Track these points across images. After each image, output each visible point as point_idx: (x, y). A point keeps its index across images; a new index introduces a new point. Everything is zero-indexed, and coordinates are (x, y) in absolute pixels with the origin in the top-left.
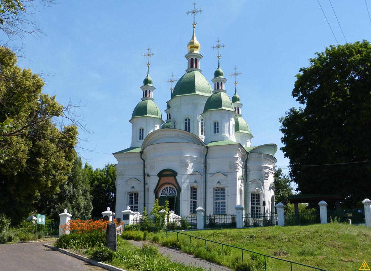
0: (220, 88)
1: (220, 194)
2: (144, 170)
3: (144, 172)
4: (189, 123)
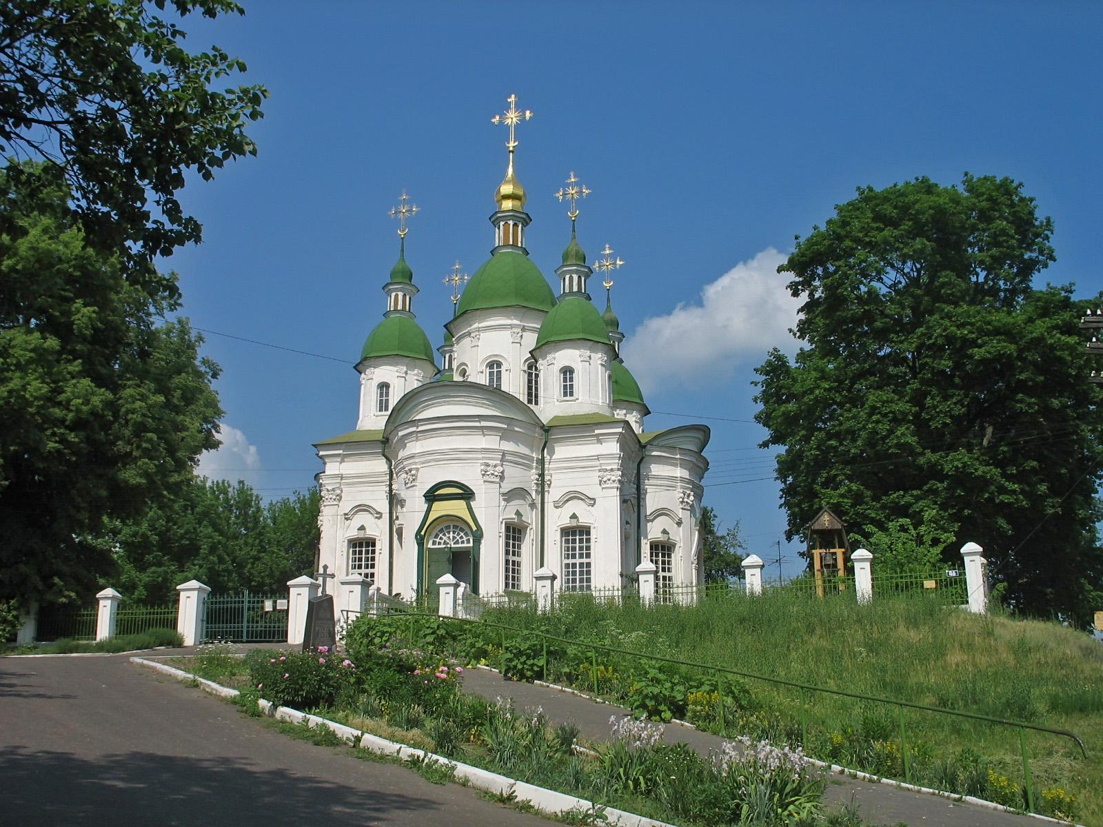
1: (577, 545)
2: (390, 485)
3: (391, 490)
4: (499, 373)
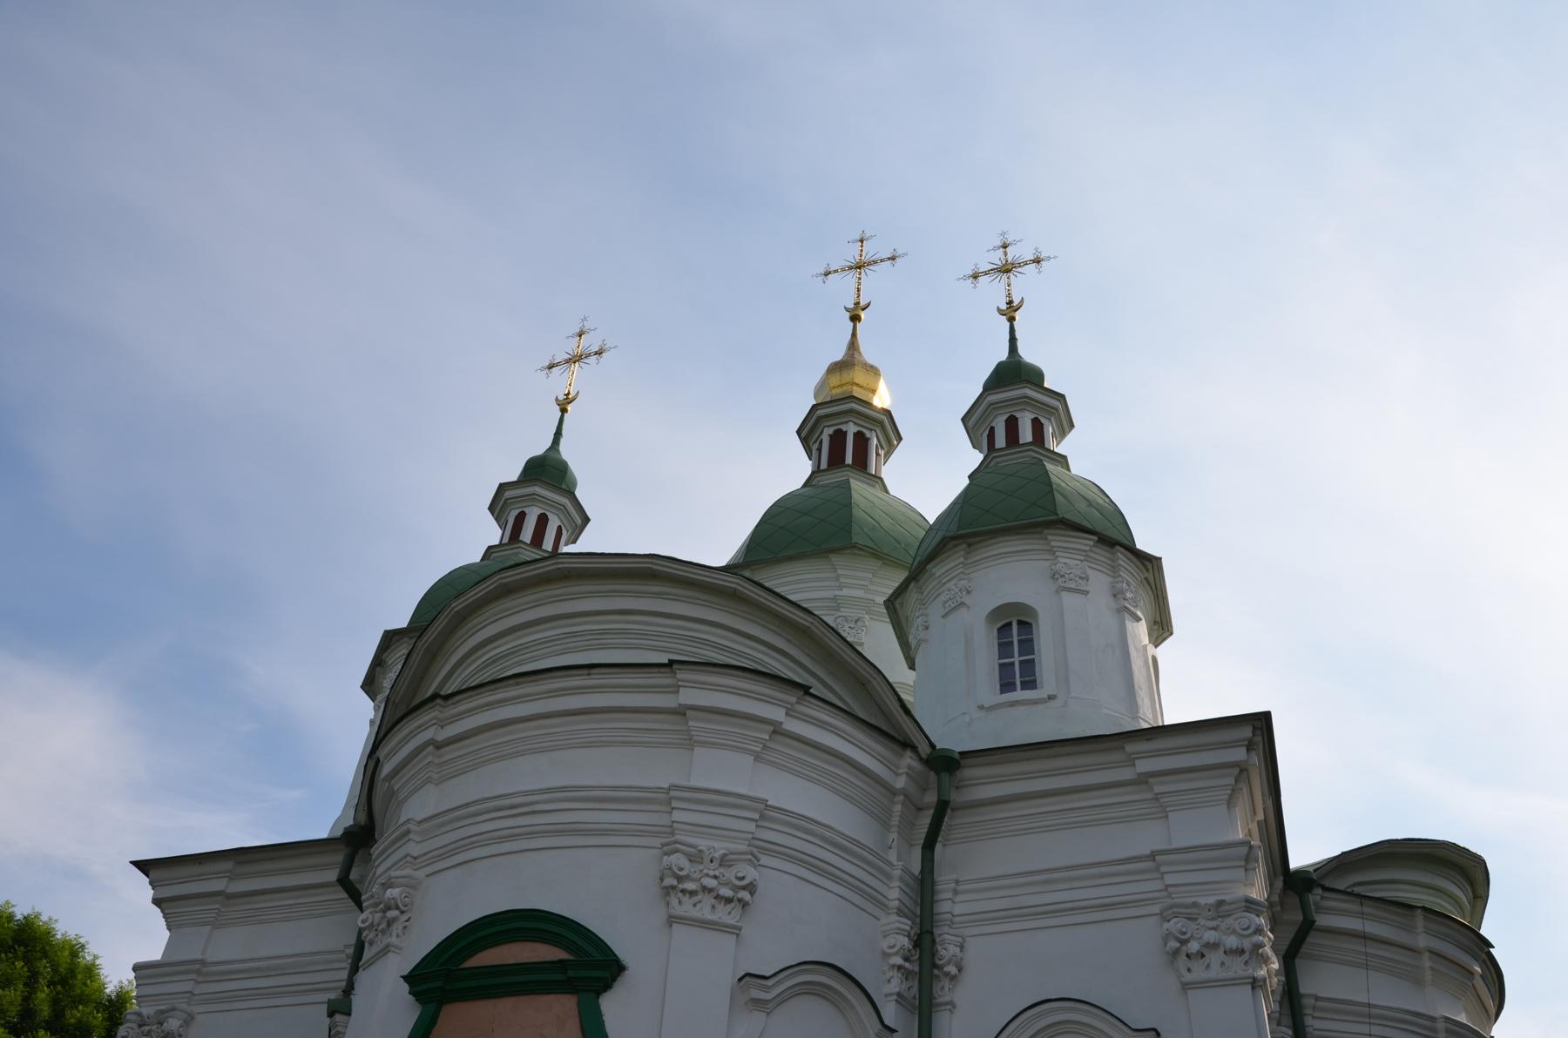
0: (1029, 438)
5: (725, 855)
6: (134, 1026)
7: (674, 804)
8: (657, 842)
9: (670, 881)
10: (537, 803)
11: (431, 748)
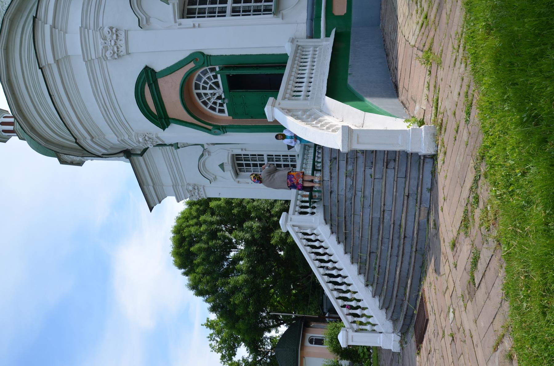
5: (102, 39)
6: (193, 197)
7: (90, 59)
8: (104, 63)
9: (116, 56)
10: (102, 103)
11: (94, 140)
